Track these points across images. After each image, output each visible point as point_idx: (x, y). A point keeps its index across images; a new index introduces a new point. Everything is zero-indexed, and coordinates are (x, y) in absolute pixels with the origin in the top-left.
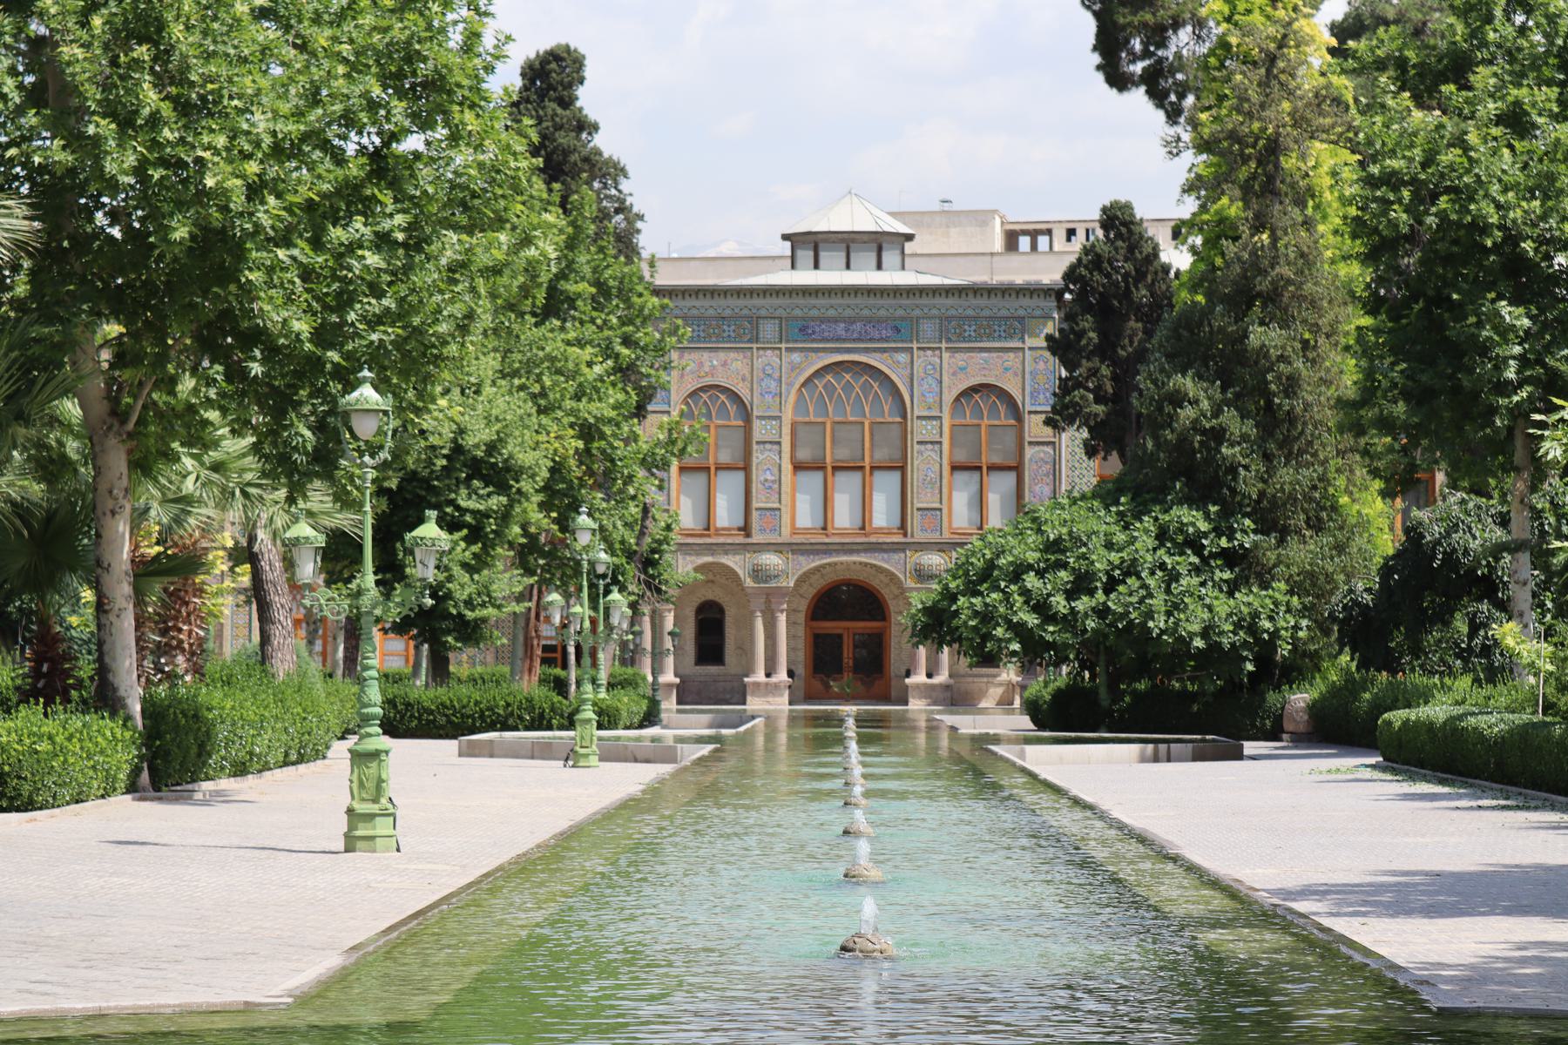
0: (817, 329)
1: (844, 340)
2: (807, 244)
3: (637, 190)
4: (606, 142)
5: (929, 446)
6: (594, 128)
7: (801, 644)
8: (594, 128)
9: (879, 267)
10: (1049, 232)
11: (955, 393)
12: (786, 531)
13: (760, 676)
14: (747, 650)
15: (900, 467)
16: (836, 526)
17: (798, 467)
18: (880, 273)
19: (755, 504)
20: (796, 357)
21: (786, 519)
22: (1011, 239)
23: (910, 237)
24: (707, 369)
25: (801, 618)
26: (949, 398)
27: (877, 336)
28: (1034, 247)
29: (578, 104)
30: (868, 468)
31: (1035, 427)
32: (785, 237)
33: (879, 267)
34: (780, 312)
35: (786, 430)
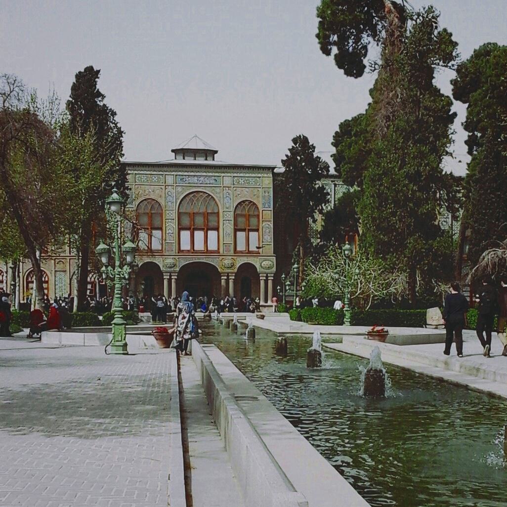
0: (187, 179)
1: (197, 183)
4: (109, 102)
5: (228, 221)
15: (217, 229)
16: (245, 250)
18: (206, 161)
20: (180, 189)
23: (216, 152)
24: (147, 192)
27: (209, 182)
29: (98, 87)
30: (206, 229)
32: (173, 151)
34: (172, 173)
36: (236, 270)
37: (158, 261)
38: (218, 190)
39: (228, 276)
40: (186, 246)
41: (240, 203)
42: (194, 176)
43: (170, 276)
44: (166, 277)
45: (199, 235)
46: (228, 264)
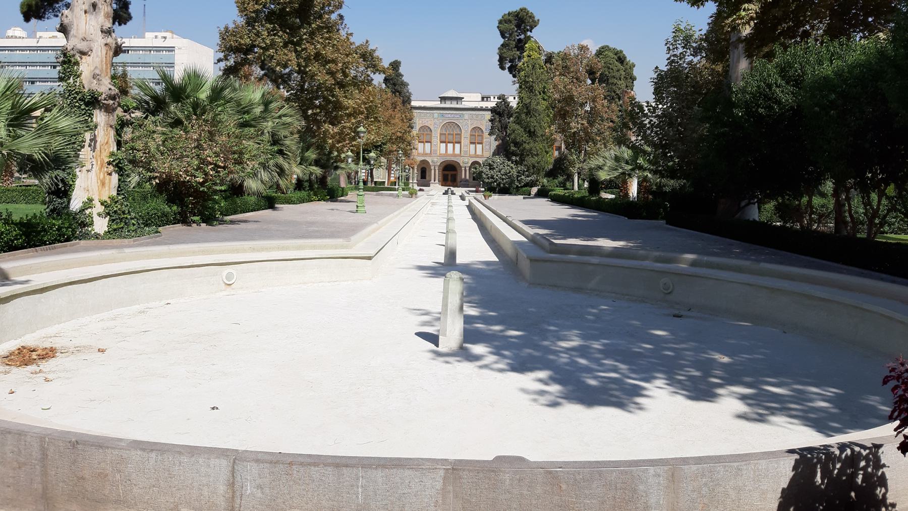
2: (443, 99)
3: (411, 89)
4: (405, 79)
6: (402, 76)
7: (441, 175)
8: (402, 76)
9: (457, 104)
10: (490, 97)
11: (471, 128)
12: (438, 154)
13: (432, 181)
14: (430, 176)
15: (459, 142)
17: (441, 142)
19: (432, 149)
21: (438, 152)
22: (483, 99)
23: (463, 98)
25: (441, 170)
26: (470, 129)
28: (487, 100)
29: (400, 71)
31: (486, 134)
32: (439, 97)
33: (457, 104)
35: (439, 135)
36: (470, 165)
37: (429, 159)
38: (461, 121)
39: (465, 168)
40: (443, 151)
41: (473, 128)
42: (449, 114)
43: (435, 167)
44: (432, 168)
45: (450, 146)
46: (465, 162)
